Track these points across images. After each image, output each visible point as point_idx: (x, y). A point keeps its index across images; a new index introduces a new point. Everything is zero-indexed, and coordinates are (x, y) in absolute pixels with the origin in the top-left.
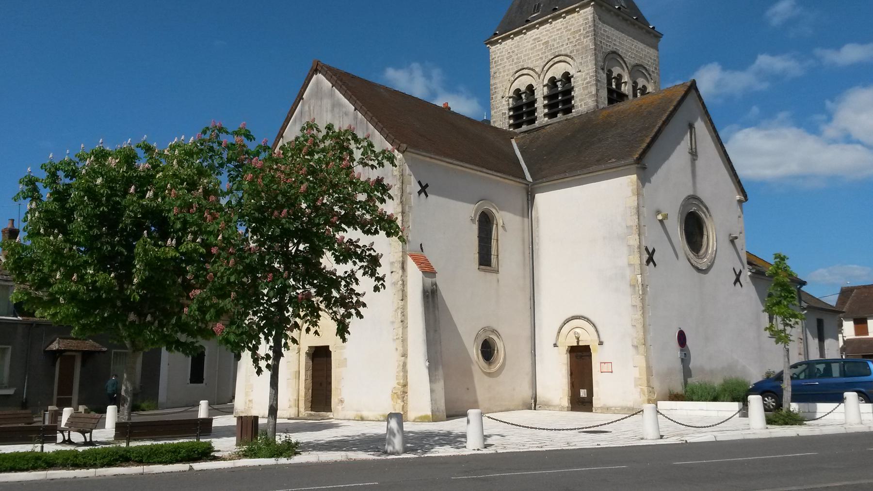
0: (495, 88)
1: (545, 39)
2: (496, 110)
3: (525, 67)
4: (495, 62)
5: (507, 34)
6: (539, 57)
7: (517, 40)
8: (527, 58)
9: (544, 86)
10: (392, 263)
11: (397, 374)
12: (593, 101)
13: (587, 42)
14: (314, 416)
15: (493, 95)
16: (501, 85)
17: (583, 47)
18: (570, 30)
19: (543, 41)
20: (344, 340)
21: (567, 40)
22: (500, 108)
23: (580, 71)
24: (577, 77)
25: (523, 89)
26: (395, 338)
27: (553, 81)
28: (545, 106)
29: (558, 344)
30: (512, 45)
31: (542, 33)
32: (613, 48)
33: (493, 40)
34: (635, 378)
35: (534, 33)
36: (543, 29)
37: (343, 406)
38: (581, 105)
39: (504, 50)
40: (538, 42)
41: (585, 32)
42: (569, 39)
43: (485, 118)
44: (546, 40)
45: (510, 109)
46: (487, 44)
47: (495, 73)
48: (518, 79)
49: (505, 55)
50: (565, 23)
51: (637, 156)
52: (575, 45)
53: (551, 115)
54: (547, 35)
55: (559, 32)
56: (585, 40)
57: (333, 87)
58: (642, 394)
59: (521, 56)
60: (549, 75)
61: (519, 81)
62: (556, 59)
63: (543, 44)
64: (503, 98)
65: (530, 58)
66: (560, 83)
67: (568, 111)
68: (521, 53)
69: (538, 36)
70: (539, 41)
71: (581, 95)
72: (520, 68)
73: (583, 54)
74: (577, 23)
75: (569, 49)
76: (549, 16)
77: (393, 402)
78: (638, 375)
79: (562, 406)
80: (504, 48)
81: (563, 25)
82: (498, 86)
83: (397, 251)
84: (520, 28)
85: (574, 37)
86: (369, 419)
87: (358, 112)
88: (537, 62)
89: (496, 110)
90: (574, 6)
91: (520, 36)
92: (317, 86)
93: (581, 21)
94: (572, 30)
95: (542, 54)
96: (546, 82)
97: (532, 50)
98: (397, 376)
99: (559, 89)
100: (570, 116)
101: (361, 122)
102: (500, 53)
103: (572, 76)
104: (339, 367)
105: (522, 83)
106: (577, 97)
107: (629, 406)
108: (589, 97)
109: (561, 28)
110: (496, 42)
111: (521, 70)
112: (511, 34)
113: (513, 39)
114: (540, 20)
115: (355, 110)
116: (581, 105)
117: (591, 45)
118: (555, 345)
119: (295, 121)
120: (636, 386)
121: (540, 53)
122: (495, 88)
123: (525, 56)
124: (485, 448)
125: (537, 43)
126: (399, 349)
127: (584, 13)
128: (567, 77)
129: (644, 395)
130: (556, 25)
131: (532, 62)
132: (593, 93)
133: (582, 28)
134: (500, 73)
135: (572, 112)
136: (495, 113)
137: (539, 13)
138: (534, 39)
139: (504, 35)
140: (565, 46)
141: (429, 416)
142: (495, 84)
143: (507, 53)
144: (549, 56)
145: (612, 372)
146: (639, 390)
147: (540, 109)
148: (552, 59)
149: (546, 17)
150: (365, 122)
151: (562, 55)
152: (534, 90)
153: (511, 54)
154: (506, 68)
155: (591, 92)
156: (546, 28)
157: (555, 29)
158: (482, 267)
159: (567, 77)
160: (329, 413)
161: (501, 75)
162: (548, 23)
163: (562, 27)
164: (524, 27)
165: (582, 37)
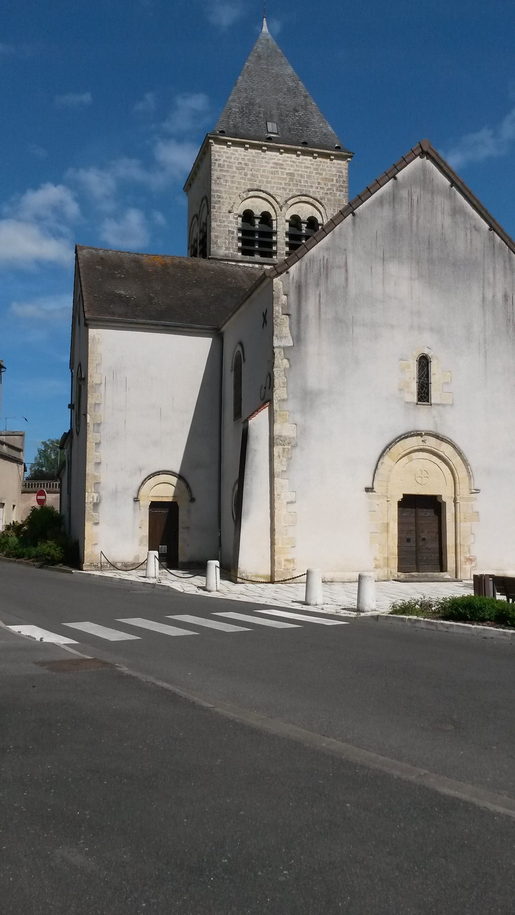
1: (289, 169)
3: (262, 189)
4: (219, 165)
7: (252, 153)
8: (265, 180)
13: (340, 195)
14: (416, 577)
15: (215, 203)
18: (321, 174)
22: (226, 223)
25: (257, 213)
31: (285, 161)
33: (221, 137)
36: (288, 157)
39: (233, 156)
40: (280, 168)
41: (338, 184)
42: (319, 183)
44: (290, 172)
47: (218, 178)
48: (250, 199)
49: (235, 163)
50: (315, 163)
52: (327, 193)
55: (308, 170)
57: (451, 186)
59: (258, 174)
60: (293, 211)
61: (252, 202)
62: (304, 198)
63: (287, 174)
64: (230, 212)
66: (306, 225)
68: (258, 170)
69: (280, 162)
70: (282, 169)
72: (256, 187)
75: (319, 194)
76: (300, 148)
82: (223, 195)
84: (260, 143)
85: (325, 184)
87: (496, 235)
90: (331, 152)
93: (334, 171)
96: (288, 217)
97: (272, 173)
99: (304, 232)
102: (227, 158)
109: (310, 168)
110: (224, 142)
112: (247, 143)
114: (288, 146)
121: (283, 182)
122: (219, 197)
123: (262, 176)
125: (280, 170)
127: (338, 164)
130: (304, 161)
131: (272, 188)
133: (335, 179)
134: (226, 181)
136: (218, 226)
139: (238, 140)
140: (314, 189)
142: (217, 191)
143: (237, 162)
147: (281, 244)
148: (299, 195)
149: (297, 147)
150: (507, 250)
151: (311, 197)
153: (243, 166)
154: (235, 179)
156: (291, 158)
157: (303, 165)
160: (442, 574)
161: (227, 184)
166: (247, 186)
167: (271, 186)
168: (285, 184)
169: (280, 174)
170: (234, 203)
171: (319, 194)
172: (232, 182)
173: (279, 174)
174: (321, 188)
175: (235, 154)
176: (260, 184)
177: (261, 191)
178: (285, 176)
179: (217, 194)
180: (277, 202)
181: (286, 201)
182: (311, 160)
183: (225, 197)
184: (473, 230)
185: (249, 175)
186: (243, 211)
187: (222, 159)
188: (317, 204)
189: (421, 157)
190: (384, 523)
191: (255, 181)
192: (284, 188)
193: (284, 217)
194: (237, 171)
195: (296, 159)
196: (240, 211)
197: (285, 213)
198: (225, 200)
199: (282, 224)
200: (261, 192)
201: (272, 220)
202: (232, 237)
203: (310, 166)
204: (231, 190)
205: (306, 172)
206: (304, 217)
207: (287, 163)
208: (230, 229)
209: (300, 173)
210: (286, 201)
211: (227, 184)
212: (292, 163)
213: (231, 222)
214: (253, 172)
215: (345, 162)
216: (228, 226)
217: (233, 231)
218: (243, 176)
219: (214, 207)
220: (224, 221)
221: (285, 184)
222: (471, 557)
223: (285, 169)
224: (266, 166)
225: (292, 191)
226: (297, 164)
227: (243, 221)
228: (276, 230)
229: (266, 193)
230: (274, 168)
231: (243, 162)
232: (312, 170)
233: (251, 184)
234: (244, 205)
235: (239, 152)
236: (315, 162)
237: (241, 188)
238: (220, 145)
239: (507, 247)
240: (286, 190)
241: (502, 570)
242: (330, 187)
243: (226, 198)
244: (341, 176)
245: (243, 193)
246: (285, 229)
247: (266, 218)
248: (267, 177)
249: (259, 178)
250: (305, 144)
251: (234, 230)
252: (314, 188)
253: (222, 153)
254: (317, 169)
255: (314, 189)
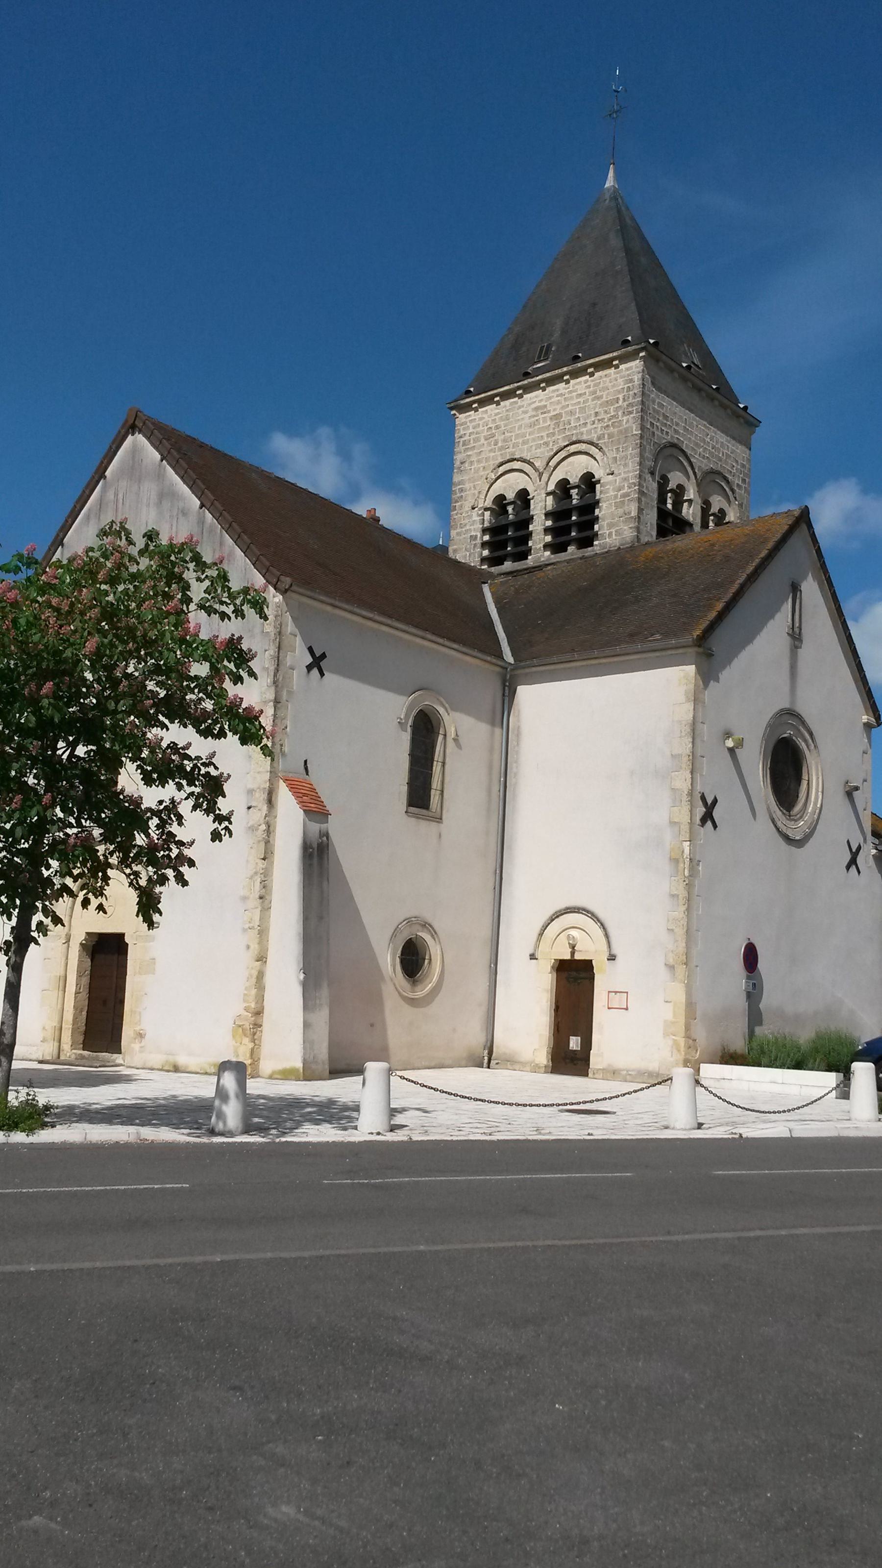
0: (461, 490)
1: (554, 410)
2: (459, 530)
3: (517, 456)
5: (489, 393)
6: (542, 442)
8: (520, 441)
9: (548, 494)
10: (250, 792)
11: (246, 992)
12: (631, 528)
13: (628, 421)
14: (86, 1059)
15: (456, 502)
16: (472, 485)
17: (621, 431)
18: (601, 397)
19: (553, 413)
20: (151, 924)
21: (593, 415)
22: (468, 527)
23: (612, 474)
24: (607, 483)
25: (510, 496)
26: (247, 926)
27: (564, 486)
28: (547, 530)
29: (538, 955)
30: (496, 415)
32: (672, 437)
33: (462, 402)
34: (665, 1021)
35: (536, 397)
36: (554, 391)
37: (142, 1044)
38: (610, 535)
39: (481, 423)
40: (542, 413)
41: (625, 404)
42: (596, 414)
43: (441, 543)
44: (555, 413)
45: (484, 531)
46: (452, 409)
47: (462, 463)
51: (698, 632)
52: (608, 426)
53: (557, 547)
54: (559, 402)
55: (581, 400)
56: (625, 418)
57: (162, 460)
58: (675, 1050)
60: (558, 475)
61: (506, 481)
62: (573, 448)
63: (551, 419)
64: (473, 508)
67: (586, 542)
69: (543, 403)
70: (545, 413)
71: (613, 516)
72: (508, 457)
73: (619, 443)
74: (613, 386)
75: (596, 432)
77: (234, 1042)
78: (669, 1016)
79: (537, 1064)
80: (481, 419)
81: (589, 387)
82: (467, 486)
83: (261, 770)
84: (512, 386)
86: (188, 1070)
87: (206, 511)
88: (538, 450)
89: (459, 530)
90: (611, 355)
91: (512, 400)
92: (133, 457)
93: (621, 384)
94: (604, 399)
95: (548, 436)
96: (551, 487)
98: (245, 995)
99: (574, 502)
100: (589, 552)
101: (211, 530)
103: (599, 482)
104: (140, 973)
105: (509, 486)
106: (604, 520)
107: (651, 1069)
108: (625, 522)
113: (498, 403)
114: (548, 375)
115: (201, 508)
116: (610, 535)
117: (634, 428)
118: (533, 957)
119: (88, 517)
120: (666, 1035)
121: (544, 434)
122: (461, 490)
123: (517, 436)
124: (391, 1131)
126: (252, 947)
127: (627, 369)
128: (589, 482)
129: (679, 1051)
130: (576, 387)
131: (529, 450)
132: (632, 515)
133: (621, 396)
134: (472, 463)
135: (592, 545)
136: (458, 534)
137: (548, 362)
138: (536, 409)
140: (589, 427)
141: (297, 1070)
142: (459, 483)
143: (486, 428)
144: (560, 441)
145: (627, 1009)
146: (670, 1042)
147: (538, 534)
151: (584, 442)
152: (529, 500)
153: (494, 431)
154: (483, 455)
155: (630, 513)
156: (558, 390)
157: (575, 394)
158: (412, 809)
159: (589, 482)
160: (115, 1055)
161: (473, 467)
162: (563, 381)
163: (587, 391)
164: (519, 384)
165: (620, 413)
166: (497, 460)
174: (599, 420)
176: (514, 450)
184: (180, 515)
185: (500, 442)
187: (468, 432)
189: (133, 435)
190: (57, 976)
191: (508, 448)
199: (540, 501)
200: (515, 462)
204: (476, 475)
206: (574, 479)
207: (553, 400)
209: (570, 408)
212: (559, 398)
214: (507, 434)
215: (638, 361)
219: (455, 508)
222: (141, 1032)
224: (523, 419)
226: (566, 396)
229: (521, 461)
231: (493, 426)
236: (592, 381)
238: (466, 412)
239: (220, 526)
241: (173, 1055)
244: (631, 387)
249: (513, 441)
253: (468, 424)
255: (589, 427)
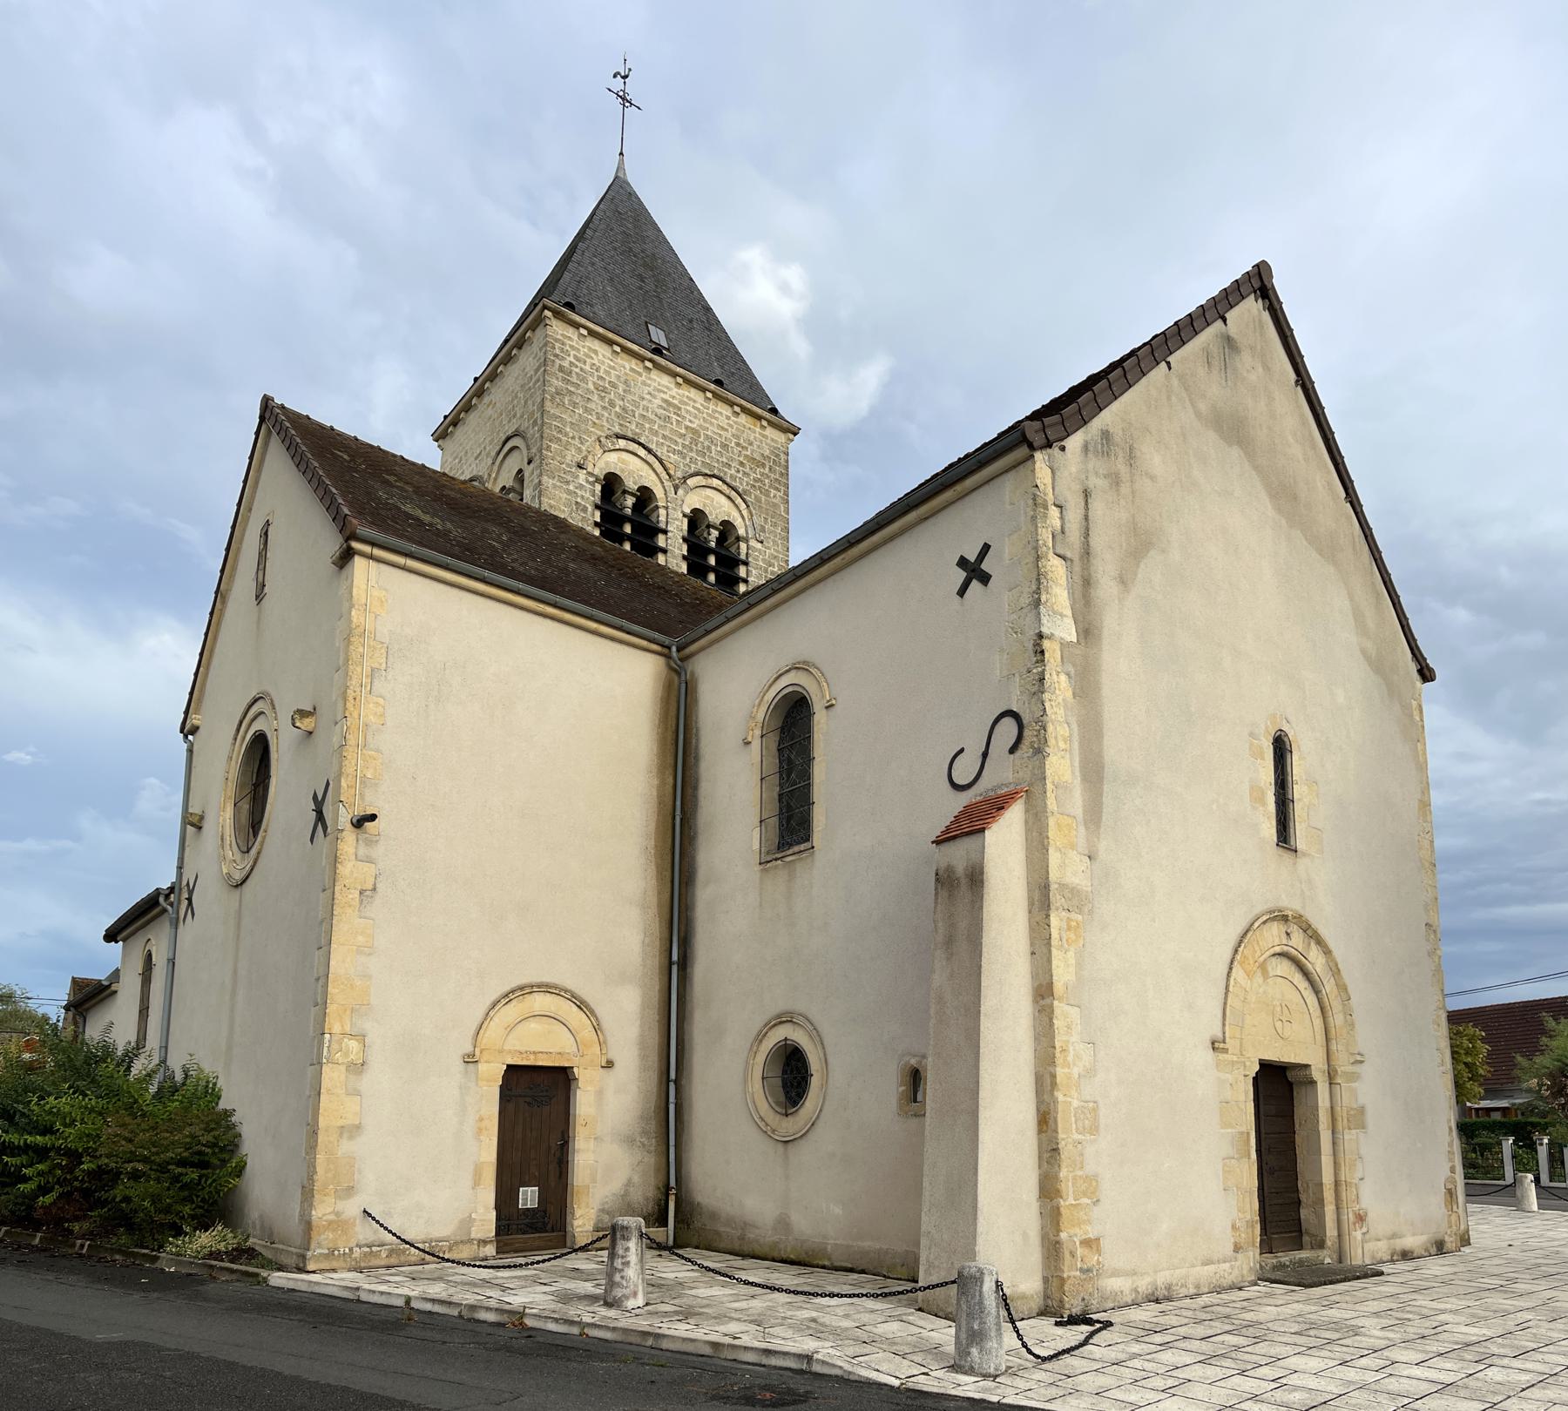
1: (690, 421)
3: (642, 441)
7: (624, 367)
25: (631, 485)
30: (610, 367)
40: (675, 413)
42: (741, 464)
50: (735, 426)
60: (693, 501)
62: (716, 482)
64: (580, 467)
65: (656, 433)
70: (678, 415)
72: (630, 434)
75: (741, 484)
85: (751, 469)
96: (688, 511)
109: (727, 430)
111: (633, 441)
130: (717, 415)
134: (575, 405)
136: (555, 486)
138: (666, 401)
147: (674, 557)
167: (657, 442)
168: (684, 446)
169: (674, 423)
170: (589, 452)
171: (741, 484)
172: (586, 410)
173: (672, 424)
174: (745, 473)
175: (593, 359)
177: (640, 444)
178: (683, 431)
179: (554, 423)
180: (668, 474)
181: (685, 479)
182: (728, 418)
183: (571, 435)
185: (618, 407)
186: (604, 473)
188: (739, 500)
192: (680, 453)
193: (681, 505)
194: (595, 391)
195: (702, 405)
196: (600, 471)
197: (683, 501)
198: (570, 440)
201: (657, 507)
202: (583, 517)
203: (726, 427)
205: (720, 436)
208: (579, 500)
209: (709, 433)
210: (685, 479)
211: (577, 411)
212: (696, 412)
213: (581, 487)
216: (575, 492)
217: (585, 506)
218: (607, 405)
220: (568, 483)
221: (684, 446)
223: (684, 418)
225: (697, 464)
226: (705, 415)
227: (602, 491)
228: (664, 527)
230: (664, 410)
232: (729, 436)
233: (621, 425)
234: (607, 463)
235: (601, 357)
236: (735, 423)
237: (602, 426)
240: (684, 458)
242: (759, 476)
243: (573, 438)
245: (606, 438)
246: (682, 530)
247: (645, 497)
248: (652, 422)
250: (719, 383)
251: (588, 505)
252: (732, 469)
254: (738, 437)
255: (733, 472)
